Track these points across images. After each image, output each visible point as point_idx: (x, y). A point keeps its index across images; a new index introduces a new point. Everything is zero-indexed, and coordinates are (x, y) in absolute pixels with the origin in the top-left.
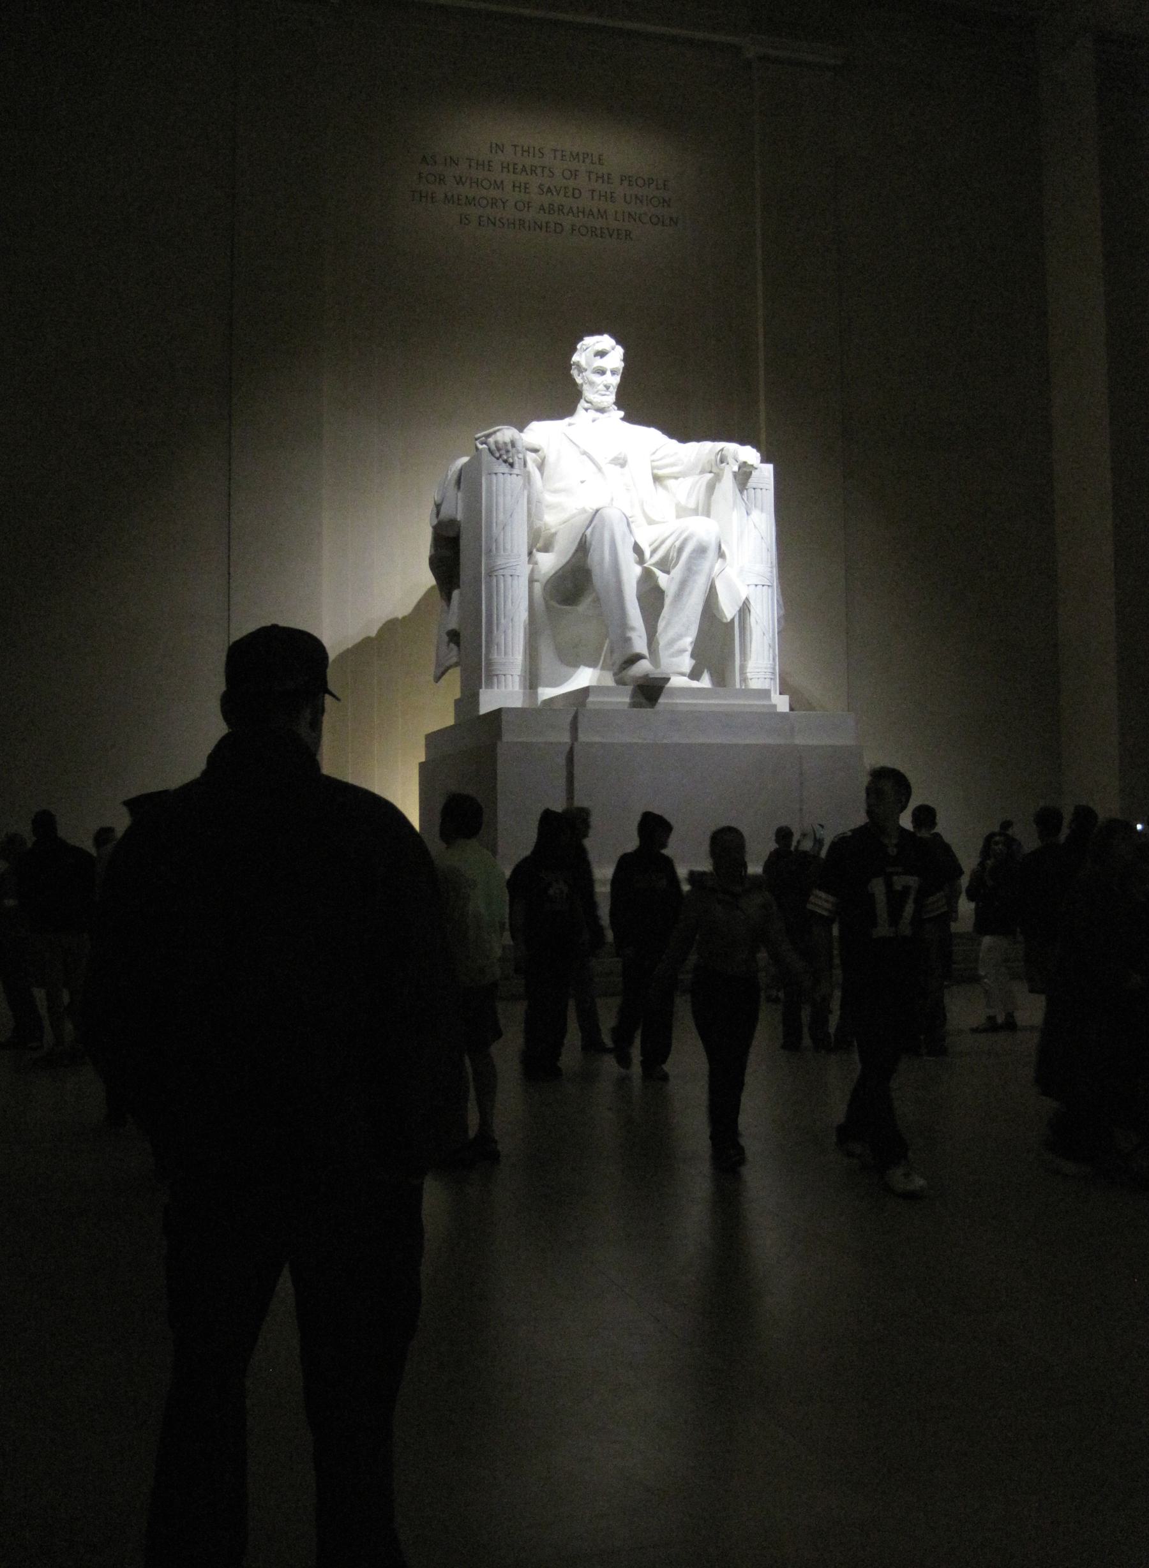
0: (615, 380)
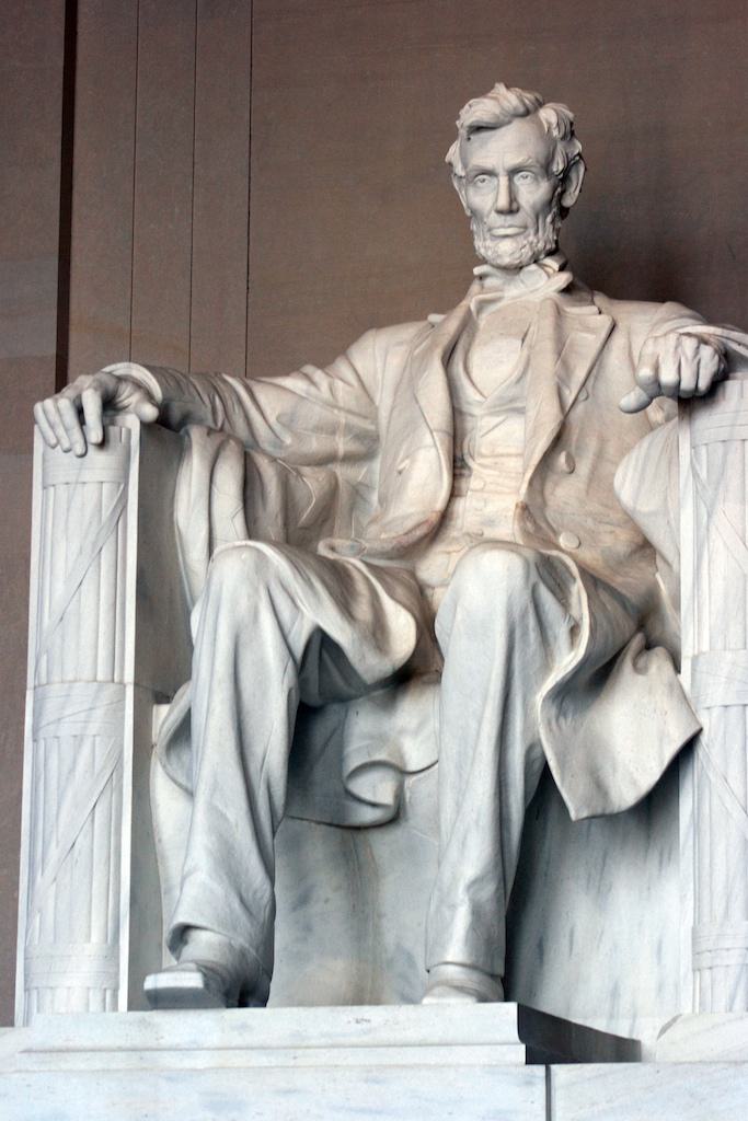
0: (532, 193)
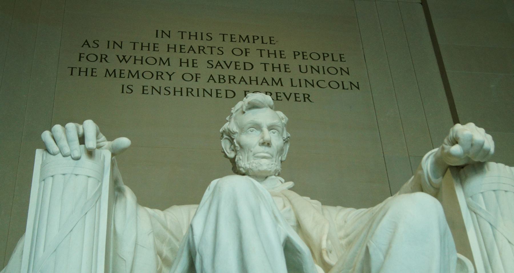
0: (277, 141)
